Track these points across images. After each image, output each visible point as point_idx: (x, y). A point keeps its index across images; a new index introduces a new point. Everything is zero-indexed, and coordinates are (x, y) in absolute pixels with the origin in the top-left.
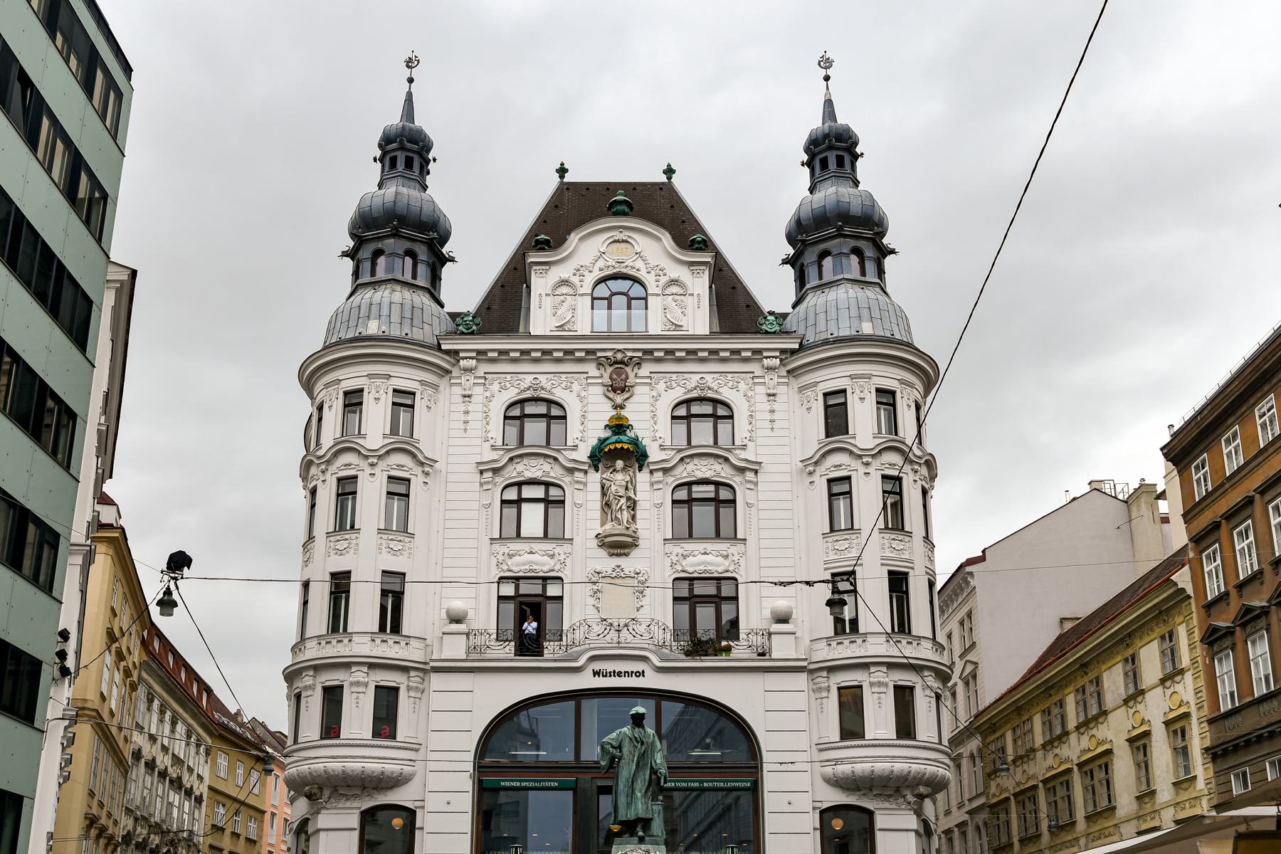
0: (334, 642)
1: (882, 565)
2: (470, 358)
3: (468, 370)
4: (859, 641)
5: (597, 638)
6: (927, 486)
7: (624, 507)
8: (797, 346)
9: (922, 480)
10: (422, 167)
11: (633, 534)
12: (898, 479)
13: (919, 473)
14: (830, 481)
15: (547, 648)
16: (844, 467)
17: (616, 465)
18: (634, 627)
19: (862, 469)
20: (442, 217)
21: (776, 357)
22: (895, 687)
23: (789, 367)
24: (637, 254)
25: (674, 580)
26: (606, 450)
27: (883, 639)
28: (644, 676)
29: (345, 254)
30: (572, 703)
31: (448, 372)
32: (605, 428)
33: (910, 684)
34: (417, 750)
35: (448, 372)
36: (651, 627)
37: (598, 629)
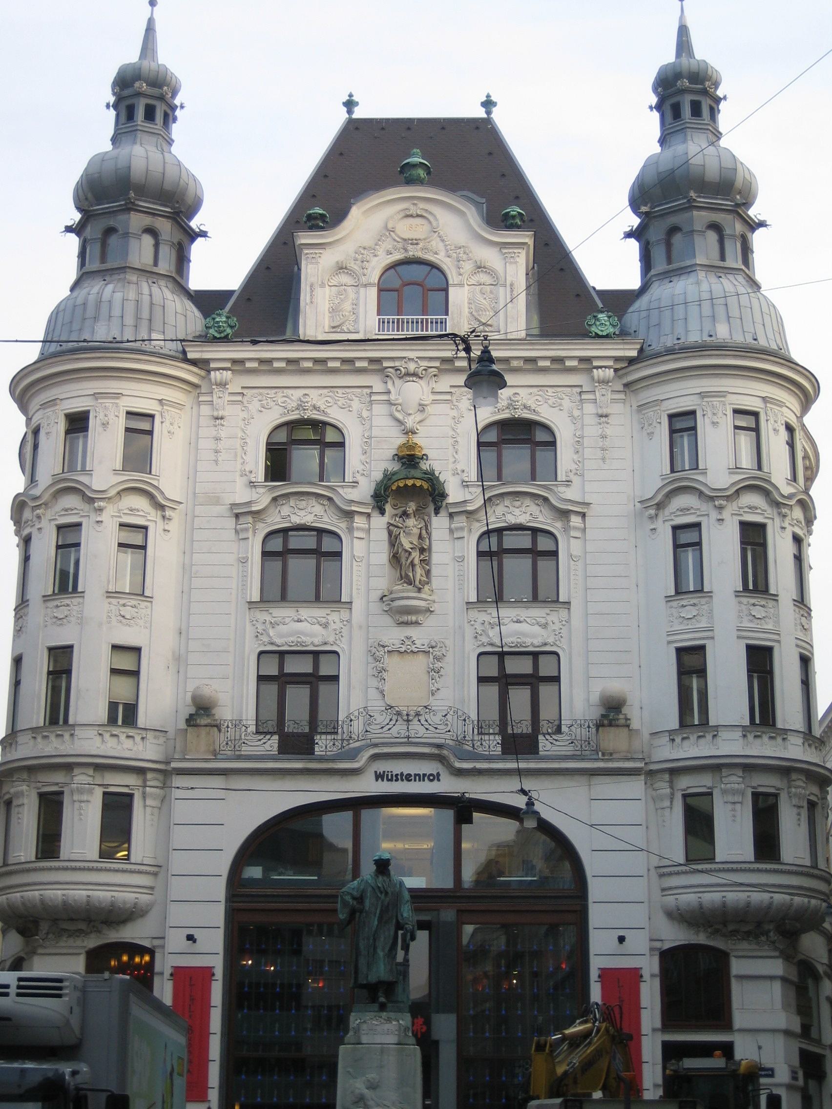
0: (52, 737)
3: (223, 385)
4: (709, 737)
6: (800, 532)
8: (634, 353)
9: (793, 526)
10: (166, 115)
12: (761, 528)
13: (789, 518)
14: (675, 528)
15: (317, 744)
18: (427, 717)
19: (714, 515)
20: (191, 183)
22: (754, 794)
23: (625, 381)
24: (435, 232)
25: (481, 654)
26: (394, 488)
27: (738, 734)
28: (439, 780)
29: (69, 229)
30: (348, 815)
33: (772, 790)
34: (155, 874)
35: (196, 386)
36: (449, 716)
37: (381, 719)
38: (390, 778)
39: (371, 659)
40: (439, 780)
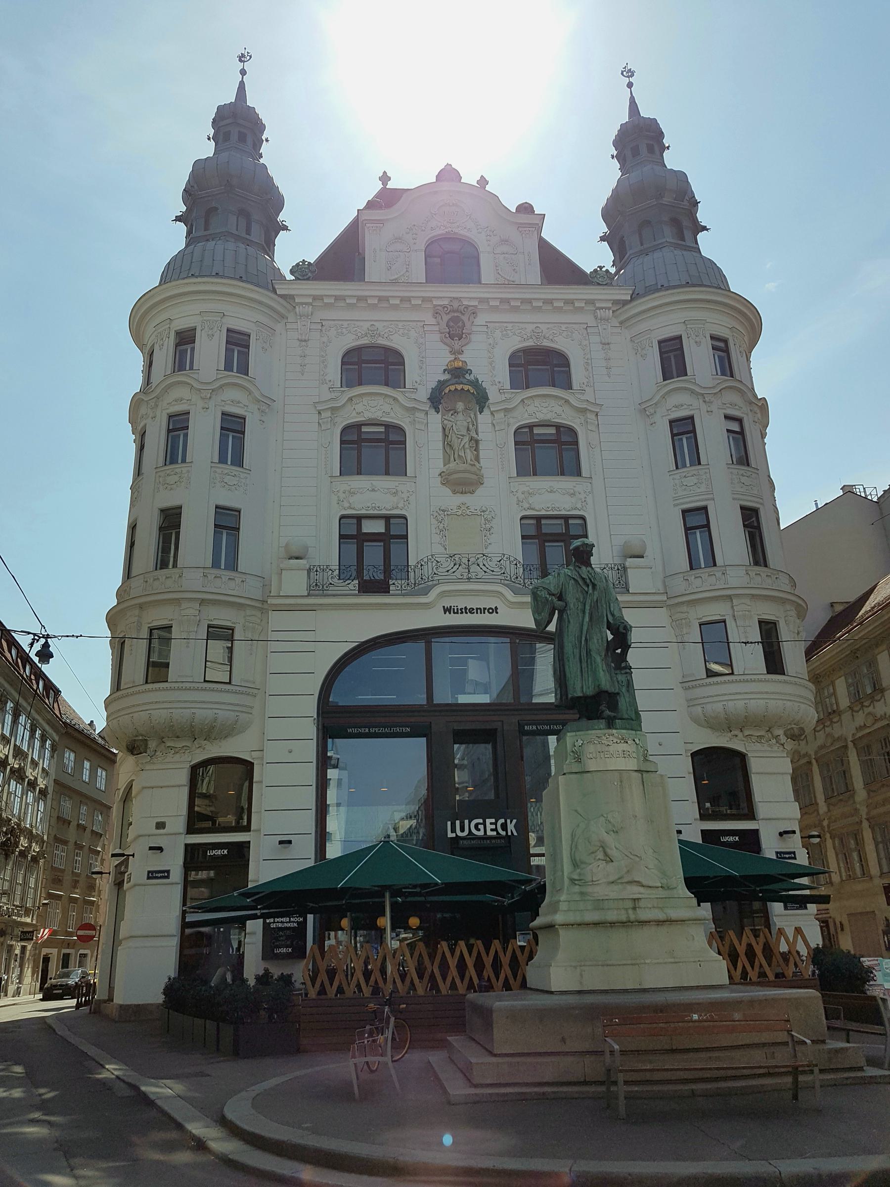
1: (734, 499)
2: (306, 304)
5: (446, 573)
7: (467, 446)
11: (478, 472)
12: (740, 421)
15: (394, 584)
16: (685, 406)
17: (458, 406)
19: (704, 407)
21: (609, 309)
23: (622, 318)
24: (468, 216)
25: (522, 518)
26: (447, 391)
27: (742, 572)
28: (497, 613)
29: (178, 219)
30: (421, 645)
31: (283, 317)
32: (444, 372)
35: (283, 317)
37: (447, 564)
38: (456, 611)
39: (434, 521)
40: (497, 613)
